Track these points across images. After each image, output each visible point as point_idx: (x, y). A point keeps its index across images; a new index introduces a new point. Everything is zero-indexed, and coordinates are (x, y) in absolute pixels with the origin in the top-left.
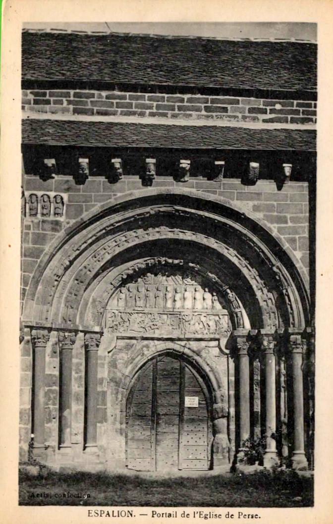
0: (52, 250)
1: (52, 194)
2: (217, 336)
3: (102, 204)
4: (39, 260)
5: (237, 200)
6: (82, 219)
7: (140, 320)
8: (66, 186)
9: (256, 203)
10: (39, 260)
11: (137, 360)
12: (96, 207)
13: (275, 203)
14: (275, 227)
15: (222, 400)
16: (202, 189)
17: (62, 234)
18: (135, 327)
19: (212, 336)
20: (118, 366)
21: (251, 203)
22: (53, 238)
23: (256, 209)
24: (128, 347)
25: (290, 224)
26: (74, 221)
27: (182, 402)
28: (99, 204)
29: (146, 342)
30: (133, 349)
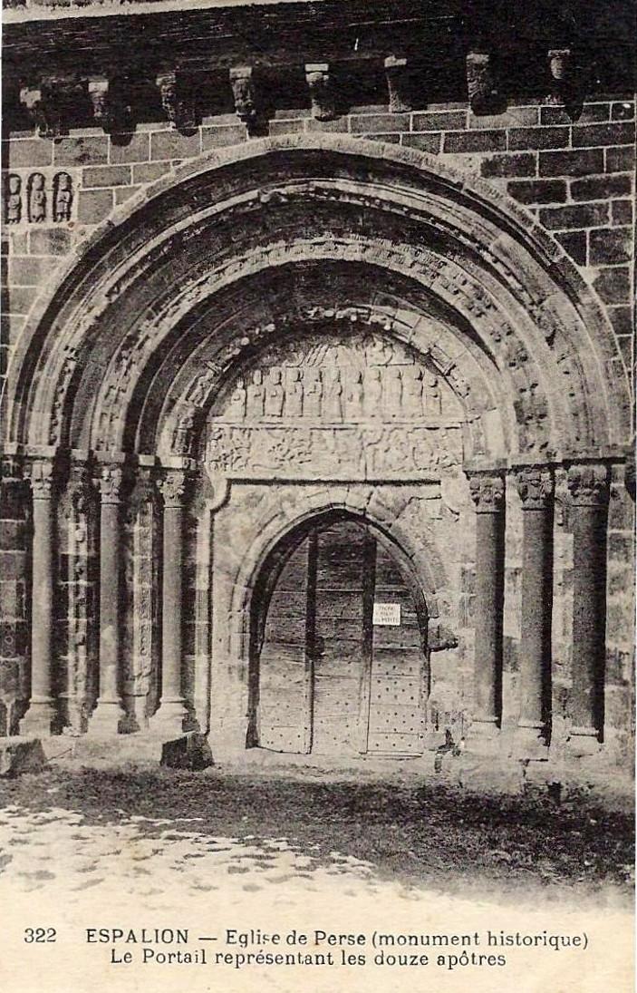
0: (52, 292)
1: (50, 171)
2: (433, 476)
3: (150, 185)
4: (27, 317)
5: (445, 151)
6: (110, 223)
7: (274, 442)
8: (77, 152)
9: (490, 155)
10: (27, 317)
11: (270, 527)
12: (138, 193)
13: (536, 153)
14: (533, 211)
15: (446, 612)
16: (365, 134)
18: (261, 461)
19: (422, 475)
20: (233, 541)
21: (478, 158)
22: (54, 268)
23: (490, 169)
24: (253, 501)
25: (570, 202)
26: (95, 228)
27: (369, 612)
28: (145, 186)
29: (287, 490)
30: (262, 503)
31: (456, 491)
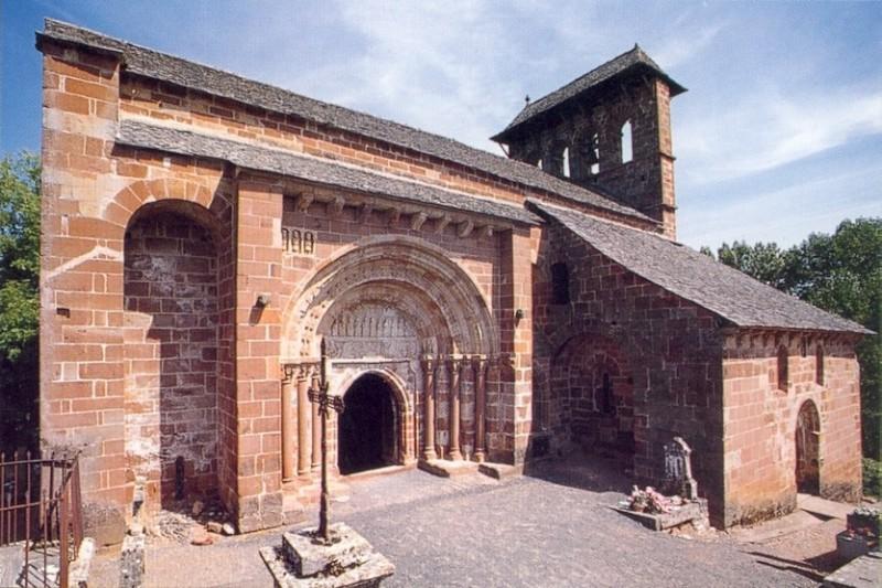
8: (317, 224)
17: (312, 272)
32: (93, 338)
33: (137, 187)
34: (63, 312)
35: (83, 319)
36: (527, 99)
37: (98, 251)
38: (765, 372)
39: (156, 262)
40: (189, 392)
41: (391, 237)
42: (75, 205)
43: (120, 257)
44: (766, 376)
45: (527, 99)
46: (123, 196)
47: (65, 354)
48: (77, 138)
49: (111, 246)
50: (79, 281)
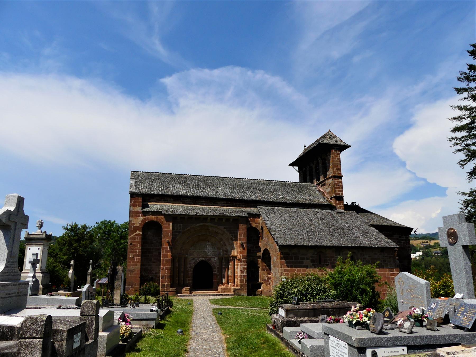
23: (225, 228)
31: (216, 259)
32: (136, 249)
33: (145, 219)
34: (131, 244)
35: (134, 245)
36: (305, 146)
37: (138, 232)
38: (308, 259)
39: (149, 233)
40: (154, 262)
41: (201, 224)
42: (134, 224)
43: (141, 233)
44: (309, 261)
45: (305, 146)
46: (142, 221)
47: (132, 252)
48: (135, 211)
49: (140, 231)
50: (133, 238)
